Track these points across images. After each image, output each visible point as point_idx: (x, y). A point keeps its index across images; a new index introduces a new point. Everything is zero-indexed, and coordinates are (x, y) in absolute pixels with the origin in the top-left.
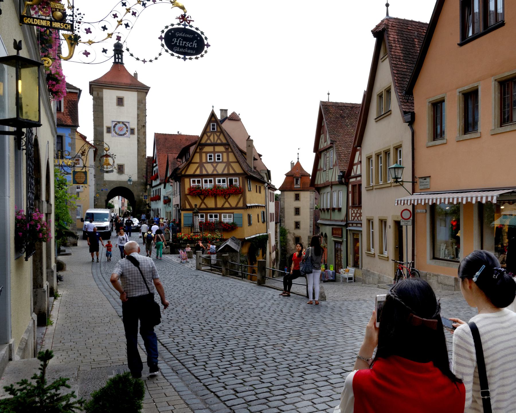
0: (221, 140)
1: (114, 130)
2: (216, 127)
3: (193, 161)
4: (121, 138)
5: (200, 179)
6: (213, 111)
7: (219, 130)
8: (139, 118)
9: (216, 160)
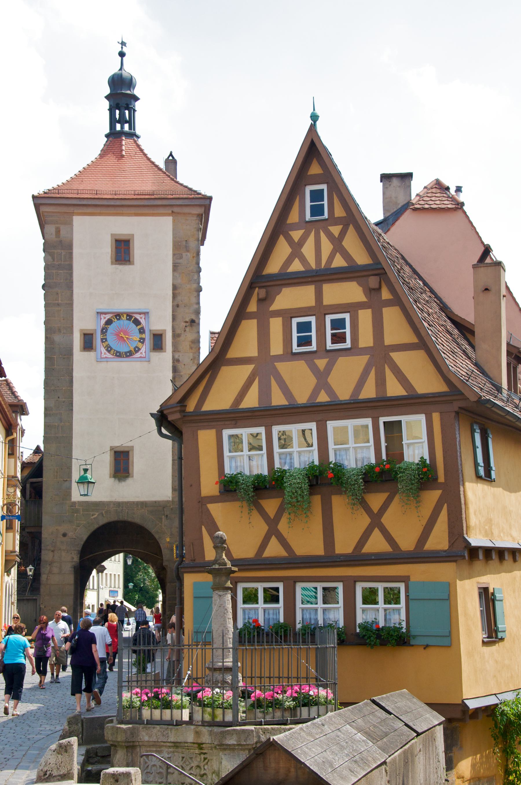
0: (346, 256)
1: (104, 340)
2: (325, 202)
3: (233, 353)
4: (124, 364)
5: (262, 430)
6: (312, 129)
7: (339, 212)
8: (179, 298)
9: (329, 345)
